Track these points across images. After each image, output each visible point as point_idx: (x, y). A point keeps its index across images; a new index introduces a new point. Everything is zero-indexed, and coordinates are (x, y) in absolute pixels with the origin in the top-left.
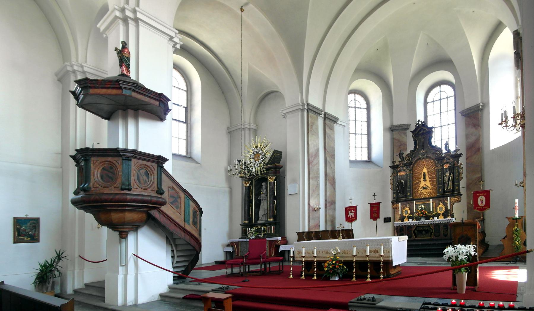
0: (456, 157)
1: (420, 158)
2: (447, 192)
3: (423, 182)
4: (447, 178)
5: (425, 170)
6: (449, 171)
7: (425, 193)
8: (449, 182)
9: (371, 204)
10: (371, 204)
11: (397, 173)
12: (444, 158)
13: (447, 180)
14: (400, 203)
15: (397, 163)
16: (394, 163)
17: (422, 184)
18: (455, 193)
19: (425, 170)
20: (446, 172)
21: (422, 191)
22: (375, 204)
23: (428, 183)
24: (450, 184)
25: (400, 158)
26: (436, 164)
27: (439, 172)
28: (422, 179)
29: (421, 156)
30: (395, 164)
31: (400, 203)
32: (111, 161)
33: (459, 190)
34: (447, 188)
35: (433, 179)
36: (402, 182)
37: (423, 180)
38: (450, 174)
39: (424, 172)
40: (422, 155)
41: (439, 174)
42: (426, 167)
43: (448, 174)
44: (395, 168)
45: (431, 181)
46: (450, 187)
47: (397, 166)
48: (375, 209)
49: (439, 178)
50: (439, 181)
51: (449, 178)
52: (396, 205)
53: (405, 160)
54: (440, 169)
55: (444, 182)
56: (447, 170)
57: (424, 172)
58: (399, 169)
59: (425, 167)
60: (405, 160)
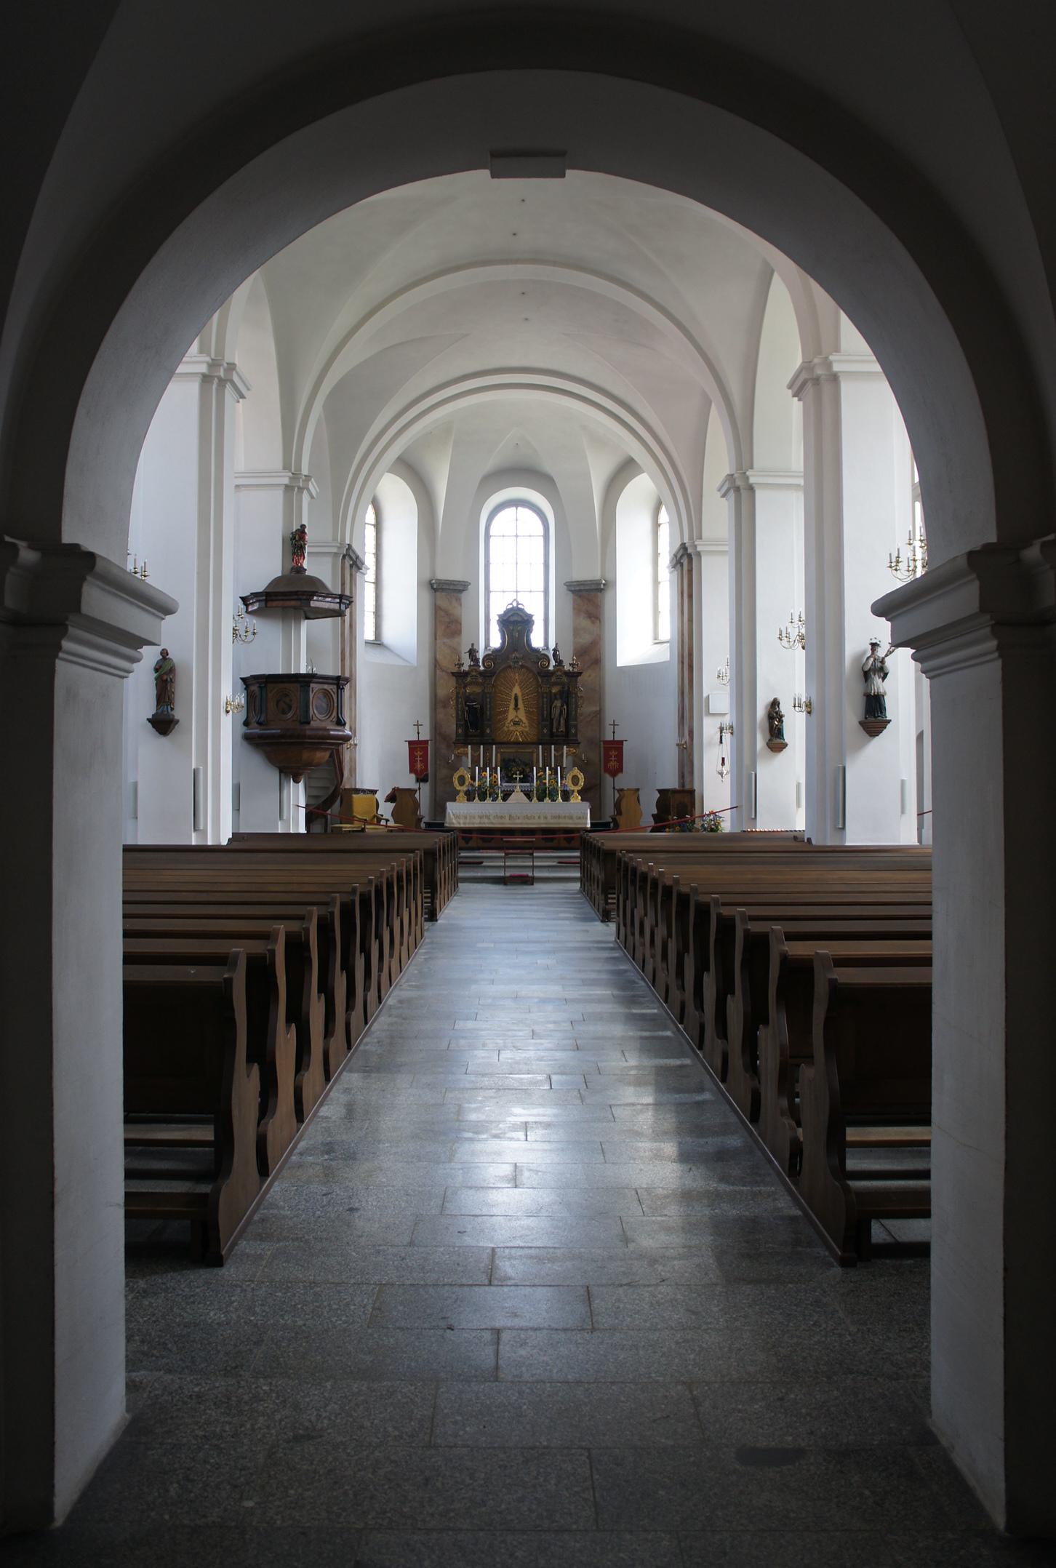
0: (572, 676)
1: (510, 667)
2: (557, 736)
3: (514, 712)
4: (558, 712)
5: (517, 690)
6: (561, 698)
7: (517, 733)
8: (560, 718)
9: (410, 743)
10: (410, 743)
11: (465, 687)
12: (552, 673)
13: (557, 715)
14: (469, 746)
15: (465, 668)
16: (459, 668)
17: (511, 715)
18: (567, 738)
19: (517, 690)
20: (556, 699)
21: (511, 728)
22: (418, 742)
23: (522, 715)
24: (562, 722)
25: (472, 660)
26: (538, 682)
27: (543, 697)
28: (512, 706)
29: (512, 664)
30: (462, 669)
31: (469, 746)
32: (328, 689)
33: (576, 735)
34: (557, 729)
35: (531, 708)
36: (477, 706)
37: (515, 709)
38: (562, 706)
39: (516, 694)
40: (515, 662)
41: (543, 702)
42: (520, 684)
43: (558, 703)
44: (461, 676)
45: (528, 713)
46: (562, 729)
47: (466, 674)
48: (419, 753)
49: (543, 708)
50: (543, 715)
51: (561, 712)
52: (462, 749)
53: (481, 664)
54: (546, 693)
55: (552, 717)
56: (558, 696)
57: (516, 694)
58: (469, 679)
59: (517, 684)
60: (481, 664)
